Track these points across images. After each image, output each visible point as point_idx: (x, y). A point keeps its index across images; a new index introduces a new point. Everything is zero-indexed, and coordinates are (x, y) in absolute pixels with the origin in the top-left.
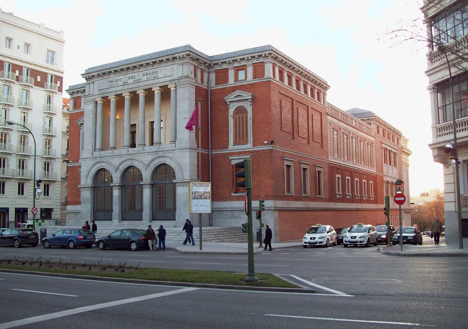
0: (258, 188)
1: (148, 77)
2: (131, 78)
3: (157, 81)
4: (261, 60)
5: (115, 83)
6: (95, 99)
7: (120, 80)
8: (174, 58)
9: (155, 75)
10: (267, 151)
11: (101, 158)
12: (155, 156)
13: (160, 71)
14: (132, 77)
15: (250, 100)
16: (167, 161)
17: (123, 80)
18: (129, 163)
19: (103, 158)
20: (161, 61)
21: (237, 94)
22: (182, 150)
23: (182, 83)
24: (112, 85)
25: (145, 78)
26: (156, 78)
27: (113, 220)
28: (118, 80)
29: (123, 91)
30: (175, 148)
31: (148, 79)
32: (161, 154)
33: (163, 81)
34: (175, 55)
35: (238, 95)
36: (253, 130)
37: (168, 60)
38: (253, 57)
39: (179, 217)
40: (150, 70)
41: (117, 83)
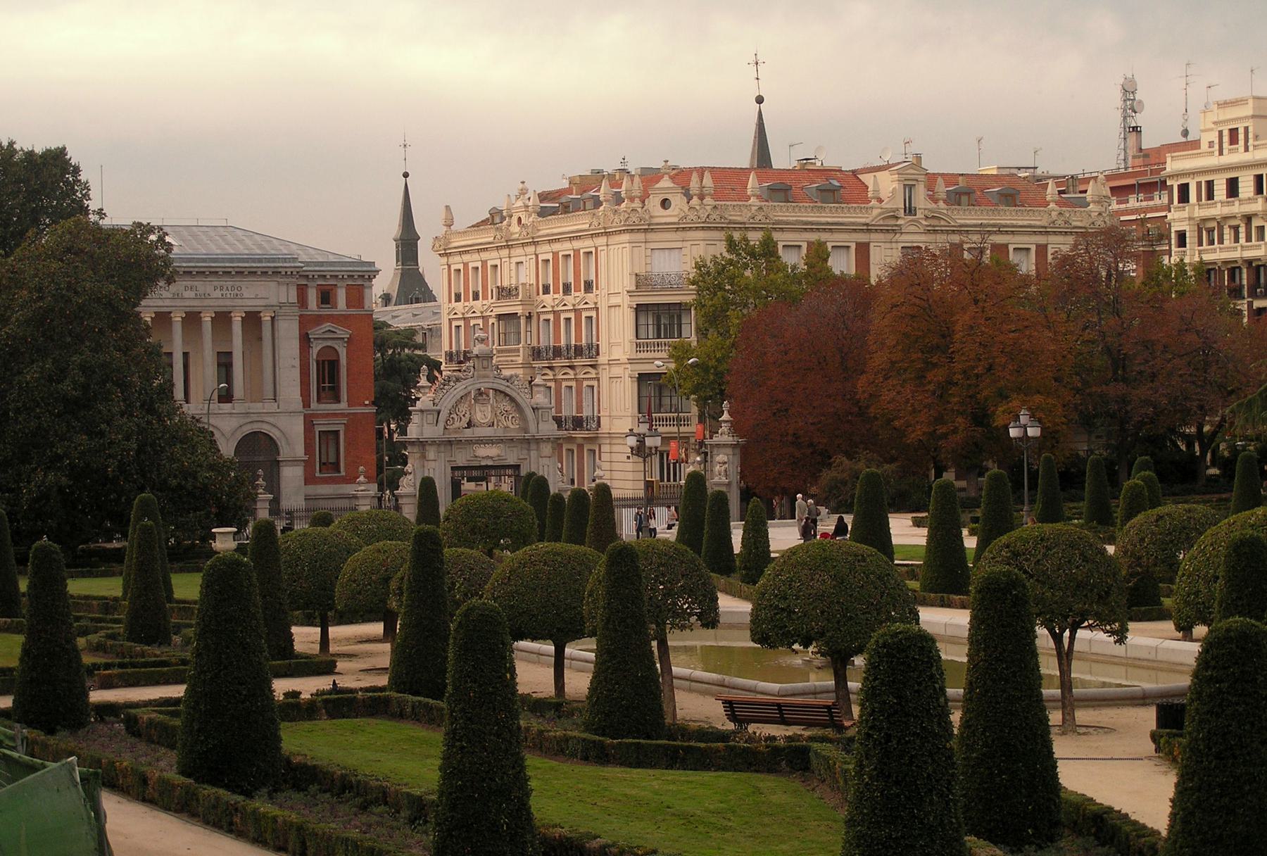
1: (224, 292)
3: (239, 302)
12: (243, 421)
16: (265, 428)
21: (327, 329)
25: (218, 293)
30: (278, 411)
34: (280, 270)
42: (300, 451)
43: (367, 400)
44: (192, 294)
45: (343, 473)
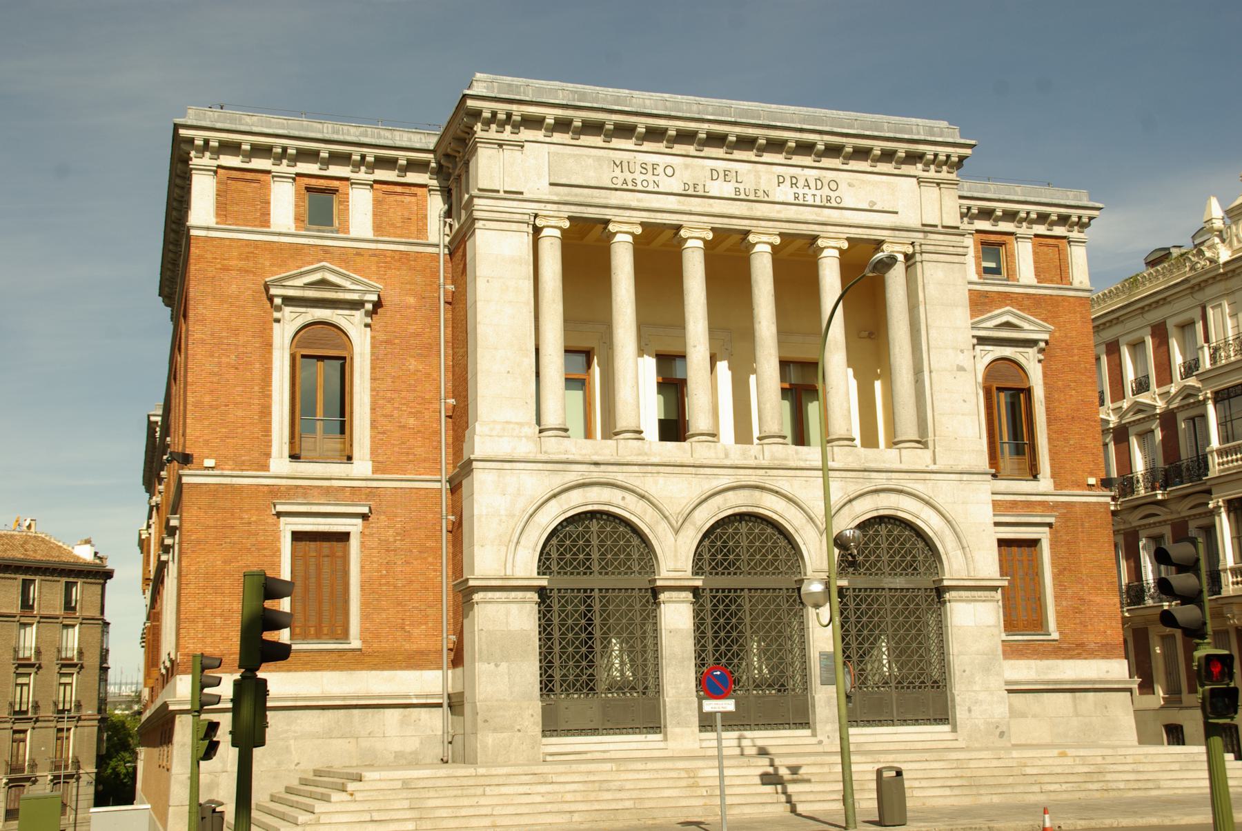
0: (1078, 621)
1: (801, 191)
2: (722, 174)
3: (834, 216)
4: (1004, 226)
5: (644, 177)
6: (536, 216)
7: (669, 171)
8: (913, 158)
9: (826, 191)
10: (1097, 507)
11: (593, 468)
13: (850, 185)
14: (725, 175)
15: (1042, 345)
17: (688, 176)
18: (739, 502)
19: (602, 468)
20: (861, 154)
22: (965, 477)
23: (942, 248)
24: (630, 183)
25: (785, 193)
26: (834, 204)
27: (671, 729)
28: (660, 170)
29: (685, 217)
30: (933, 467)
31: (801, 202)
32: (880, 480)
33: (866, 224)
35: (1008, 325)
36: (1050, 439)
37: (888, 156)
38: (1042, 218)
39: (970, 711)
40: (805, 170)
41: (656, 178)
42: (987, 565)
43: (1092, 474)
44: (728, 190)
45: (1055, 636)
